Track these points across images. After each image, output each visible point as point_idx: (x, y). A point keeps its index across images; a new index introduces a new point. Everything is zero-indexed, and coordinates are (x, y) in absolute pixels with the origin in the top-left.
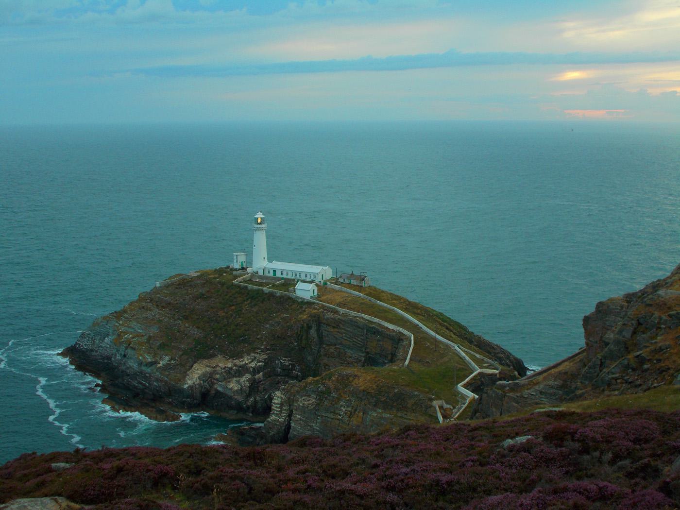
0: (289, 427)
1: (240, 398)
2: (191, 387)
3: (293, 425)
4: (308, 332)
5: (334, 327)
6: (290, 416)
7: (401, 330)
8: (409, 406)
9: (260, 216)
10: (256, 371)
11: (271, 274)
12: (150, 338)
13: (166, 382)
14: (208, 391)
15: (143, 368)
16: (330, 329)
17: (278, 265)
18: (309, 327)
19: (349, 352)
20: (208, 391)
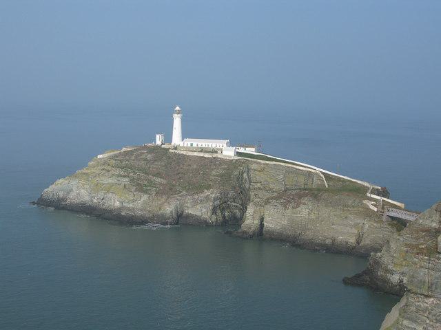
0: (262, 226)
1: (206, 216)
2: (171, 212)
3: (265, 224)
4: (242, 174)
5: (260, 171)
6: (262, 220)
7: (310, 170)
8: (350, 204)
9: (178, 108)
10: (215, 199)
11: (189, 145)
12: (125, 185)
13: (149, 211)
14: (182, 214)
15: (124, 204)
16: (257, 172)
17: (188, 142)
18: (243, 173)
19: (271, 186)
20: (182, 214)
